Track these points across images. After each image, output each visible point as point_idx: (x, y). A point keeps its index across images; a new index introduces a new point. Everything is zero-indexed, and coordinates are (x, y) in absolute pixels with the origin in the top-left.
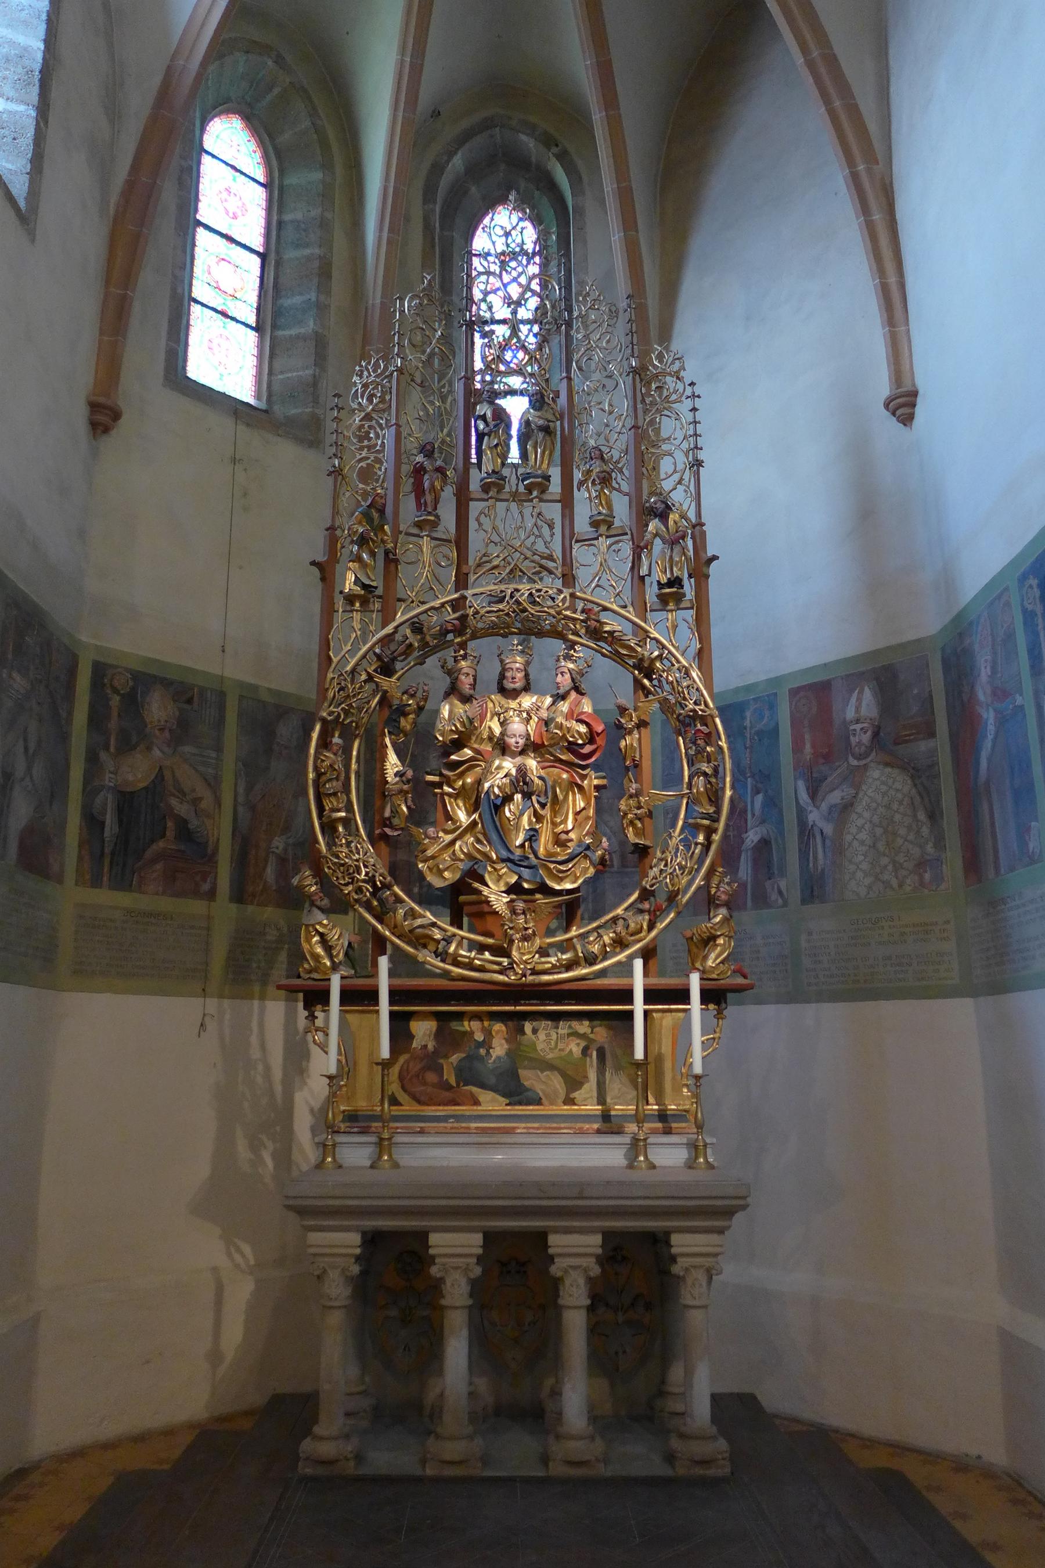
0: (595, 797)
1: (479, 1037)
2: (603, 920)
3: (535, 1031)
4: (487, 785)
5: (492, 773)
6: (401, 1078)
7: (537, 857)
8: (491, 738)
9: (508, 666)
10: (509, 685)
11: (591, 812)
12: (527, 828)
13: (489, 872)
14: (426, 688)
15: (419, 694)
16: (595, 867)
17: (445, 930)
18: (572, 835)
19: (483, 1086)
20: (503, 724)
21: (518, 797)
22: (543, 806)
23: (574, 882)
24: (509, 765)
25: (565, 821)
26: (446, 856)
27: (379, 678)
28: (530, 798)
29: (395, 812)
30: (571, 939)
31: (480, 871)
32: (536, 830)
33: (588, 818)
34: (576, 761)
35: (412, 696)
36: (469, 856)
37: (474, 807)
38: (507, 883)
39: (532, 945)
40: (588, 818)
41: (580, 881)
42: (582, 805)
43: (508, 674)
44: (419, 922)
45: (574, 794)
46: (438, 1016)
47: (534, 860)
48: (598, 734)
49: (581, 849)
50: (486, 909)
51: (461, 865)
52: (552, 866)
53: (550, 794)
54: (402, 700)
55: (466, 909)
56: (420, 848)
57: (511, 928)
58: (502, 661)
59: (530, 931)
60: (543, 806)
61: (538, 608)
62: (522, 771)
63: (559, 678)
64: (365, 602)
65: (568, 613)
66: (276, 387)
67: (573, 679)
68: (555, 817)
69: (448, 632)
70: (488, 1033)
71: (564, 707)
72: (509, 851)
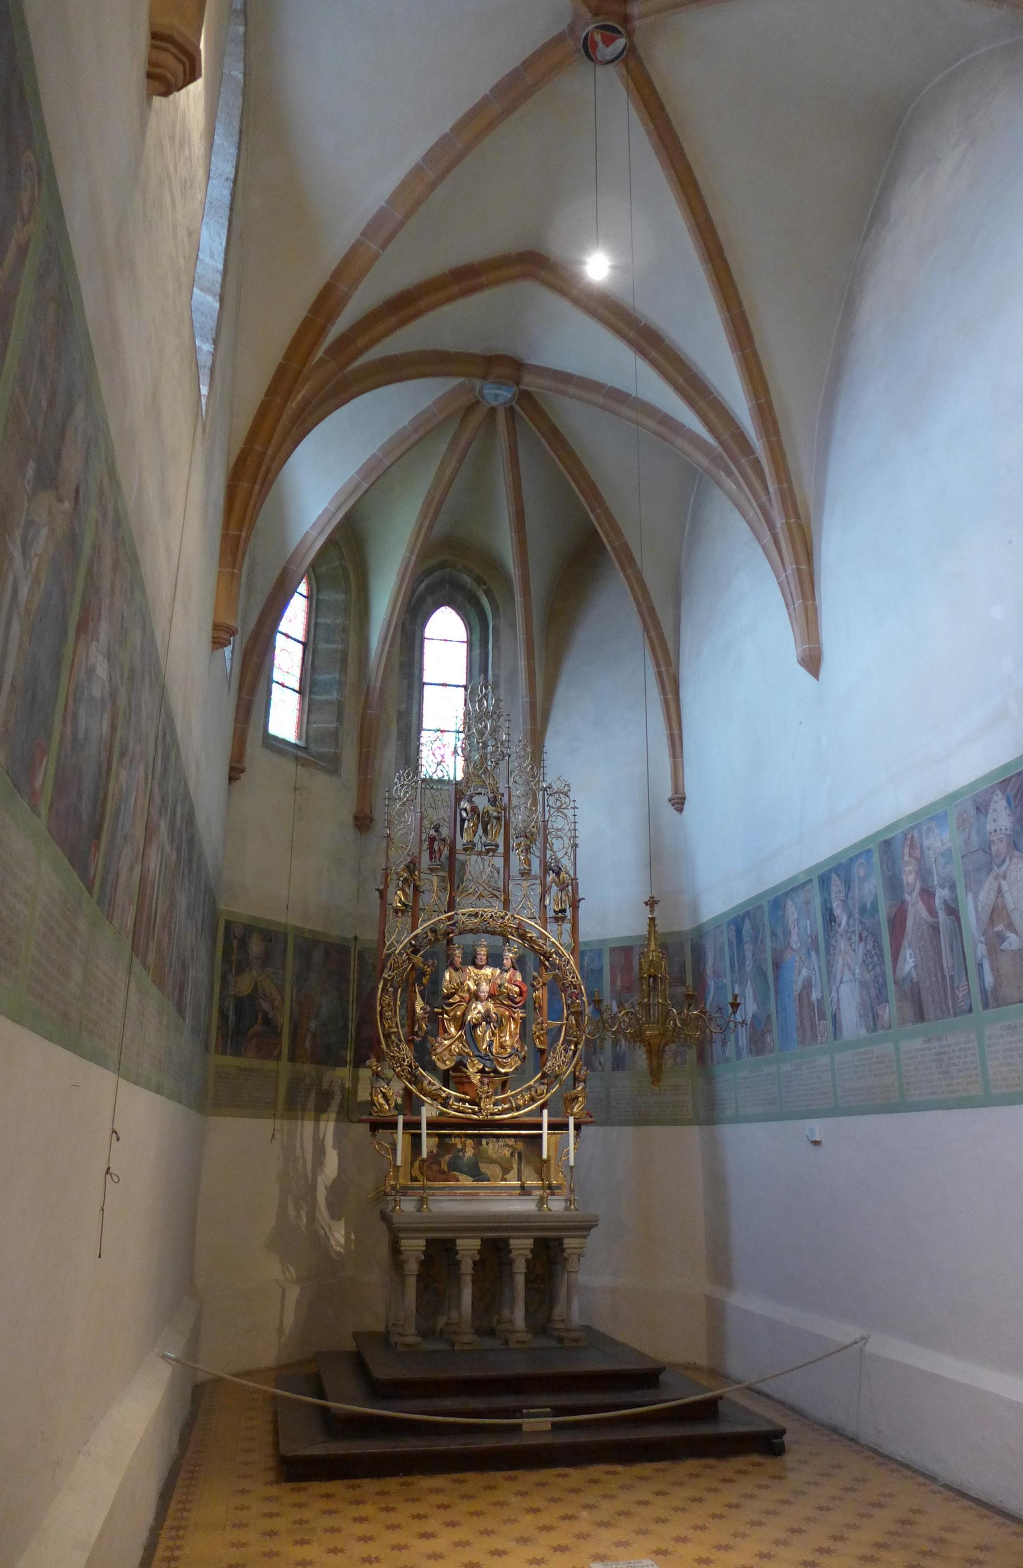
1: (459, 1146)
3: (487, 1144)
4: (469, 1018)
6: (420, 1168)
19: (461, 1172)
20: (478, 985)
27: (412, 956)
29: (420, 1028)
46: (439, 1135)
50: (465, 1080)
62: (488, 1011)
64: (403, 912)
66: (311, 732)
70: (464, 1145)
71: (507, 976)
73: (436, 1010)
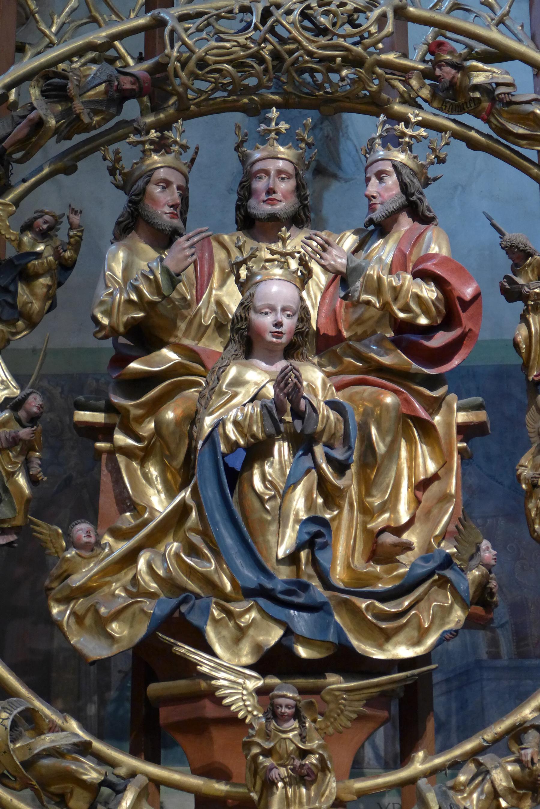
0: (461, 451)
2: (489, 735)
4: (208, 421)
5: (222, 394)
7: (328, 585)
9: (258, 166)
10: (260, 208)
12: (303, 516)
13: (216, 622)
14: (76, 219)
15: (62, 234)
17: (112, 764)
18: (410, 536)
21: (282, 450)
22: (341, 468)
24: (258, 377)
25: (391, 504)
28: (309, 451)
30: (412, 781)
31: (194, 619)
32: (325, 523)
33: (445, 498)
34: (415, 367)
35: (44, 235)
37: (182, 474)
38: (257, 647)
39: (320, 794)
40: (445, 498)
41: (431, 641)
42: (432, 467)
43: (260, 185)
44: (48, 740)
45: (411, 442)
47: (319, 591)
48: (466, 305)
49: (431, 565)
50: (210, 710)
51: (149, 606)
53: (356, 444)
54: (20, 243)
55: (166, 715)
56: (55, 571)
57: (267, 753)
58: (244, 159)
59: (313, 759)
60: (341, 468)
61: (323, 40)
62: (290, 388)
63: (374, 187)
65: (391, 57)
67: (404, 187)
68: (369, 494)
69: (124, 96)
71: (385, 250)
73: (84, 416)
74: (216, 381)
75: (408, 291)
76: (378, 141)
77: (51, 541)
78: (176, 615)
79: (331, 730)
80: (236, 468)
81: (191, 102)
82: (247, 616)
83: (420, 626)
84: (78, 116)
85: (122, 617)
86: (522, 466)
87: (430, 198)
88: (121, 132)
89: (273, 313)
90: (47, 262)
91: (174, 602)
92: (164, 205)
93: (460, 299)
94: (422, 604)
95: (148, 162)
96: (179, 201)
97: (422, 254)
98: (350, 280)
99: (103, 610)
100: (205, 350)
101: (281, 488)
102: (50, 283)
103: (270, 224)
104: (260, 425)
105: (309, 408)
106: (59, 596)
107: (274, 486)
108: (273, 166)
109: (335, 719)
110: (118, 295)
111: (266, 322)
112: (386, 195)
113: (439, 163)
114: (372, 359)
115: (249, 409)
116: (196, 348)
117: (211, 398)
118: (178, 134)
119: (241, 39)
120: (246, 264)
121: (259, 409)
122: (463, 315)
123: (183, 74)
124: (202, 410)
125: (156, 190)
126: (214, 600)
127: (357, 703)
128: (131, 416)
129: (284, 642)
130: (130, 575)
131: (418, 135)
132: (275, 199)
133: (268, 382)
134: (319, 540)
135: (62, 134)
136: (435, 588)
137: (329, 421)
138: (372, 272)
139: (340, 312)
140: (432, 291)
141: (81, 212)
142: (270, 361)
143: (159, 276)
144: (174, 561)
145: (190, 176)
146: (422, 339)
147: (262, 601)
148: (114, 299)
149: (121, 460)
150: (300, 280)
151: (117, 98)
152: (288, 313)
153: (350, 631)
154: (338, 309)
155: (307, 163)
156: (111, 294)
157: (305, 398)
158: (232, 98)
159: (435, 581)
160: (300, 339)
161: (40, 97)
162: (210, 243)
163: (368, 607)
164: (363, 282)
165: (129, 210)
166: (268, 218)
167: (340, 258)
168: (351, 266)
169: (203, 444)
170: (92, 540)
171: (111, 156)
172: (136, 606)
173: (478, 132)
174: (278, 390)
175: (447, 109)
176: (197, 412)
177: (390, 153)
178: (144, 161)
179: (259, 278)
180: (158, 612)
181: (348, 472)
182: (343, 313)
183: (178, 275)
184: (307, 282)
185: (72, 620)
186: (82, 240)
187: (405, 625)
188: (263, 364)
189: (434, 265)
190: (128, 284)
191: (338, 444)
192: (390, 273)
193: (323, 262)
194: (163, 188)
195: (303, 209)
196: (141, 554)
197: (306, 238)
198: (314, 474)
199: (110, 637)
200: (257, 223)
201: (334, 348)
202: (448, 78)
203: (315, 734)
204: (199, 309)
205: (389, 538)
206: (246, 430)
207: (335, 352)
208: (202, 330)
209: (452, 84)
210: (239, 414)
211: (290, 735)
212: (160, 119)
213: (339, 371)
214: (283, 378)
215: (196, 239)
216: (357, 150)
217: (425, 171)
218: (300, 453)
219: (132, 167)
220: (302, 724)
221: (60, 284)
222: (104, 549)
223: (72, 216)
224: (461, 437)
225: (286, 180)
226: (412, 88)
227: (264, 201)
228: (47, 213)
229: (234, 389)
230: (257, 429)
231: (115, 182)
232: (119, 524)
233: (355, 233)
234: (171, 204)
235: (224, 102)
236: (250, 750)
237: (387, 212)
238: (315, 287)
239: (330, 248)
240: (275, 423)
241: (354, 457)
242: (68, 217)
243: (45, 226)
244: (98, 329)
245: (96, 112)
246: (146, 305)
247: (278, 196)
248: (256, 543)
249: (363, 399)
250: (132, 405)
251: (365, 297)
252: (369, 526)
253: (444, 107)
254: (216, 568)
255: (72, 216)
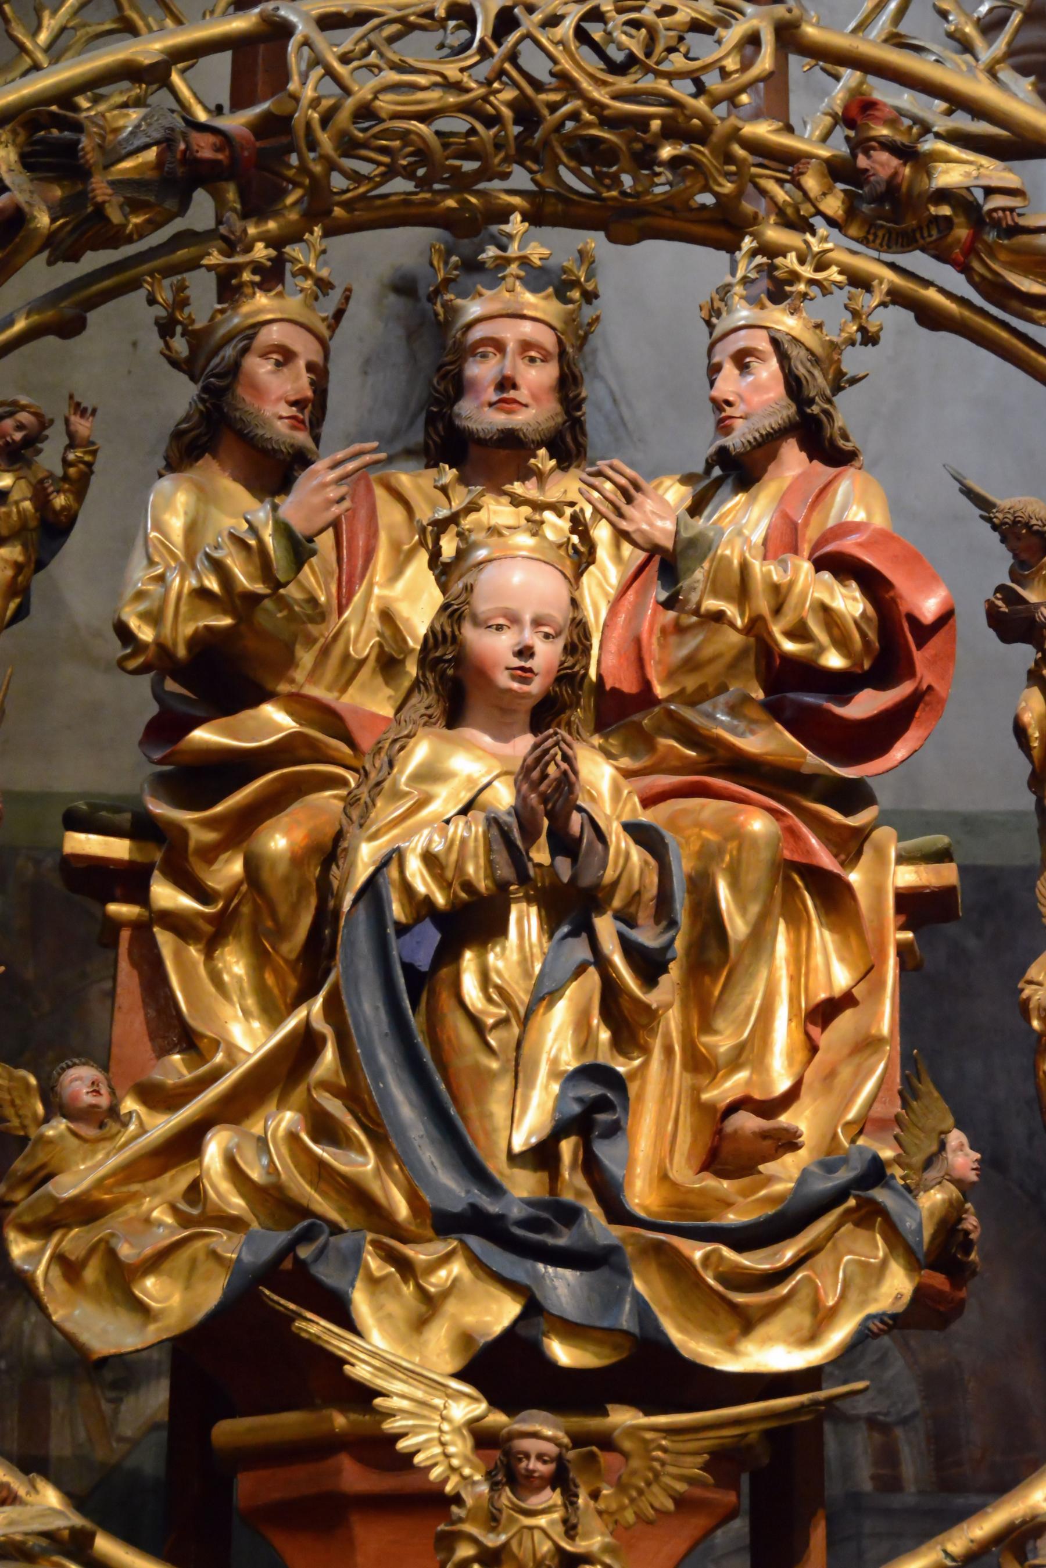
4: (366, 855)
5: (397, 795)
7: (617, 1212)
8: (388, 664)
9: (478, 333)
11: (886, 1019)
12: (569, 1062)
14: (82, 426)
15: (50, 457)
16: (914, 1262)
18: (799, 1119)
21: (525, 922)
22: (650, 966)
23: (812, 1339)
24: (473, 770)
25: (752, 1051)
26: (157, 1210)
28: (585, 928)
31: (327, 1274)
33: (867, 1044)
34: (813, 761)
36: (273, 1201)
40: (867, 1044)
41: (838, 1336)
42: (842, 978)
43: (482, 371)
48: (924, 632)
49: (844, 1175)
50: (354, 1477)
51: (228, 1245)
52: (697, 1252)
55: (248, 1488)
61: (624, 83)
63: (729, 383)
65: (762, 130)
67: (794, 386)
68: (707, 1027)
72: (474, 1170)
74: (386, 768)
75: (804, 595)
76: (739, 289)
77: (13, 1103)
78: (288, 1264)
79: (629, 1516)
80: (417, 964)
81: (337, 198)
82: (443, 1273)
83: (816, 1306)
84: (99, 210)
85: (166, 1266)
86: (1030, 982)
87: (848, 413)
88: (182, 254)
89: (515, 628)
90: (19, 512)
91: (282, 1237)
92: (278, 400)
93: (913, 620)
94: (820, 1259)
95: (245, 309)
96: (309, 393)
97: (831, 523)
98: (682, 565)
99: (125, 1251)
100: (356, 711)
101: (522, 1002)
102: (21, 559)
103: (503, 453)
104: (482, 861)
105: (589, 834)
106: (27, 1219)
107: (506, 998)
108: (512, 332)
109: (641, 1492)
110: (178, 580)
111: (496, 647)
112: (756, 399)
113: (864, 343)
114: (719, 741)
115: (458, 829)
116: (334, 704)
117: (374, 805)
118: (312, 255)
119: (452, 71)
120: (457, 524)
121: (480, 830)
122: (918, 656)
123: (324, 138)
124: (352, 830)
125: (260, 368)
126: (370, 1236)
127: (689, 1460)
128: (192, 844)
129: (522, 1331)
130: (184, 1182)
131: (826, 279)
132: (515, 401)
133: (497, 777)
134: (602, 1117)
135: (62, 248)
136: (848, 1227)
137: (629, 865)
138: (728, 552)
139: (650, 644)
140: (855, 599)
141: (94, 411)
142: (502, 735)
143: (269, 541)
144: (284, 1151)
145: (333, 345)
146: (828, 700)
147: (474, 1242)
148: (167, 590)
149: (164, 939)
150: (573, 563)
151: (180, 175)
152: (546, 629)
153: (665, 1311)
154: (645, 636)
155: (581, 332)
156: (161, 579)
157: (580, 810)
158: (422, 196)
159: (849, 1212)
160: (566, 692)
161: (18, 167)
162: (370, 491)
163: (706, 1259)
164: (709, 572)
165: (201, 407)
166: (499, 440)
167: (662, 518)
168: (685, 535)
169: (356, 901)
170: (104, 1101)
171: (164, 295)
172: (199, 1244)
173: (942, 290)
174: (525, 787)
175: (878, 241)
176: (339, 836)
177: (764, 313)
178: (239, 307)
179: (482, 554)
180: (247, 1258)
181: (664, 979)
182: (655, 646)
183: (310, 540)
184: (581, 574)
185: (56, 1272)
186: (92, 472)
187: (785, 1301)
188: (487, 739)
189: (860, 545)
190: (200, 556)
191: (644, 916)
192: (765, 558)
193: (624, 525)
194: (278, 364)
195: (572, 428)
196: (209, 1135)
197: (590, 474)
198: (592, 977)
199: (142, 1310)
200: (474, 451)
201: (636, 717)
202: (884, 174)
203: (596, 1523)
204: (345, 623)
205: (747, 1122)
206: (449, 874)
207: (638, 726)
208: (351, 667)
209: (892, 185)
210: (436, 838)
211: (542, 1521)
212: (268, 231)
213: (645, 768)
214: (538, 760)
215: (351, 466)
216: (615, 401)
217: (836, 357)
218: (565, 929)
219: (212, 319)
220: (570, 1498)
221: (40, 565)
222: (125, 1125)
223: (75, 419)
224: (902, 919)
225: (538, 363)
226: (805, 194)
227: (491, 405)
228: (23, 408)
229: (425, 787)
230: (476, 871)
231: (167, 352)
232: (157, 1076)
233: (687, 479)
234: (292, 398)
235: (406, 203)
236: (451, 1551)
237: (757, 435)
238: (596, 590)
239: (638, 497)
240: (518, 859)
241: (679, 945)
242: (67, 421)
243: (18, 436)
244: (129, 651)
245: (134, 206)
246: (238, 602)
247: (522, 394)
248: (464, 1118)
249: (701, 826)
250: (194, 821)
251: (712, 604)
252: (705, 1096)
253: (871, 237)
254: (377, 1169)
255: (75, 419)
